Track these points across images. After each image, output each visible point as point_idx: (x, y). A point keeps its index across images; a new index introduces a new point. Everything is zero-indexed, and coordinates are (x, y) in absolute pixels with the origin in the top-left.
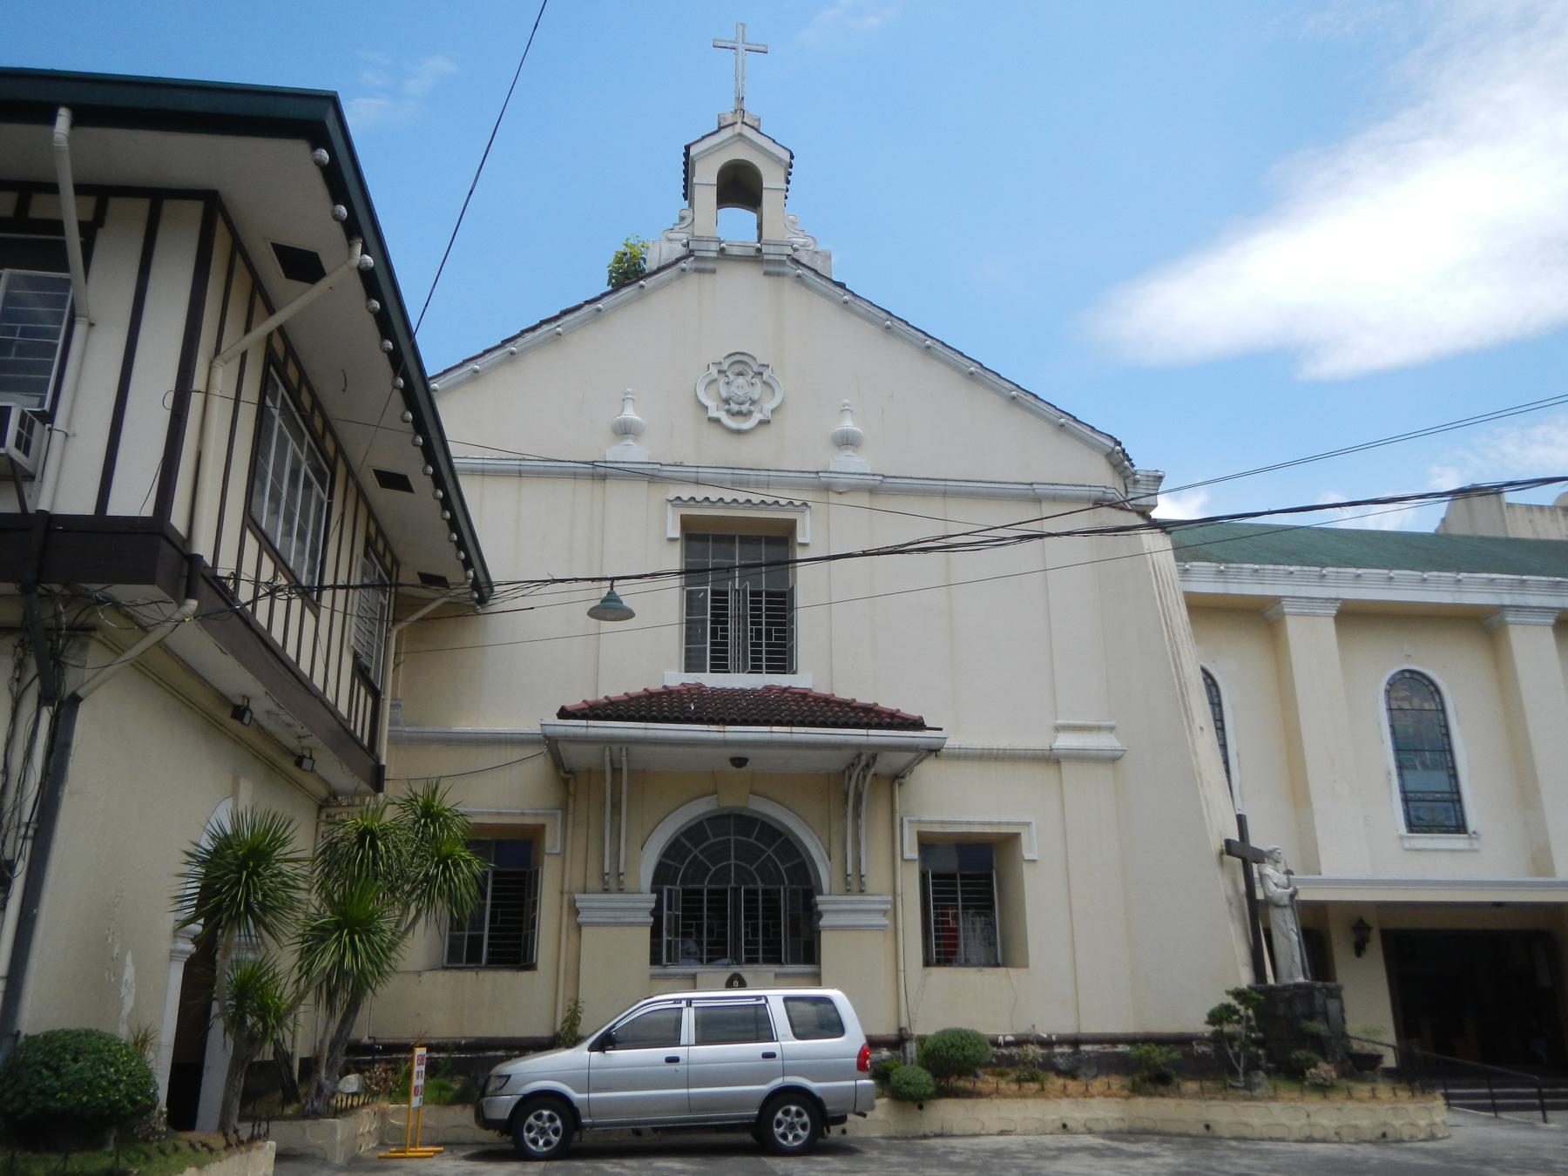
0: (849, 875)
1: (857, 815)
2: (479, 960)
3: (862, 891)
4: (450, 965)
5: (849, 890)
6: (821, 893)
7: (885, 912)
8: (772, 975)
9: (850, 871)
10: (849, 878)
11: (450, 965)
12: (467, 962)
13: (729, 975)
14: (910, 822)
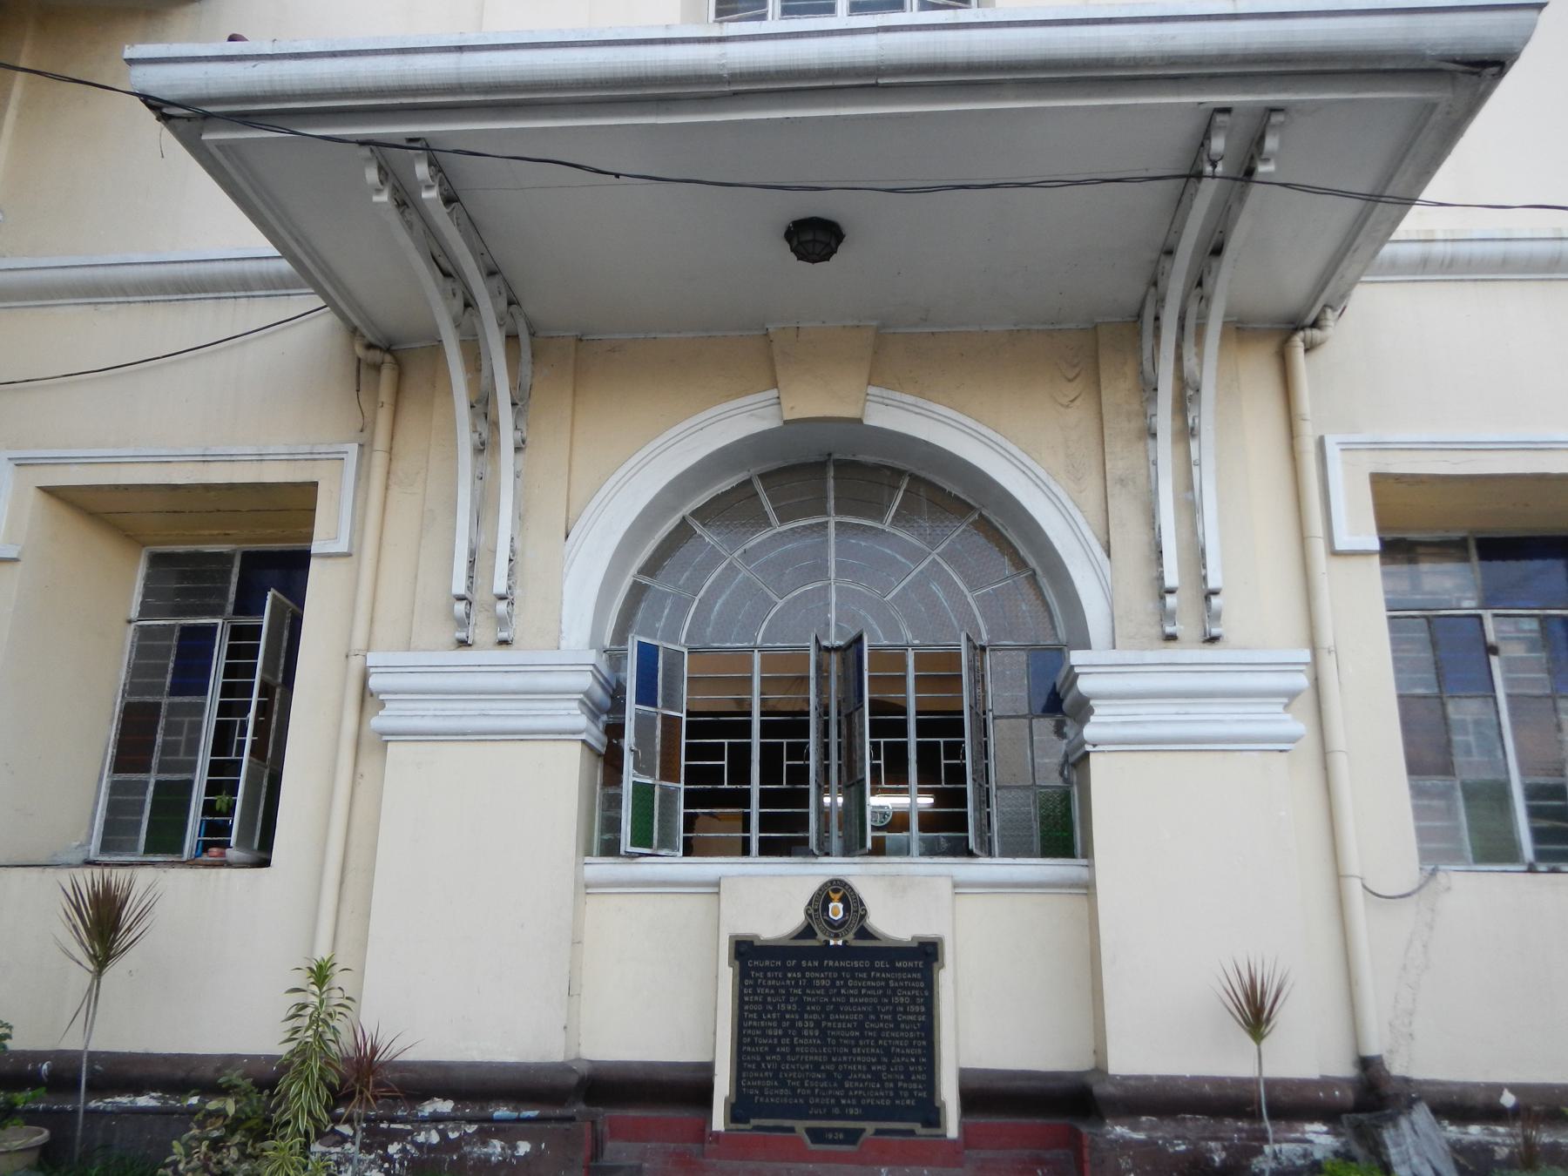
0: (1171, 591)
1: (1186, 433)
2: (177, 848)
3: (1213, 640)
4: (105, 858)
5: (1171, 638)
6: (1086, 645)
7: (1290, 697)
8: (946, 886)
9: (1171, 580)
10: (1171, 600)
11: (105, 858)
12: (147, 851)
13: (813, 886)
14: (1347, 448)
